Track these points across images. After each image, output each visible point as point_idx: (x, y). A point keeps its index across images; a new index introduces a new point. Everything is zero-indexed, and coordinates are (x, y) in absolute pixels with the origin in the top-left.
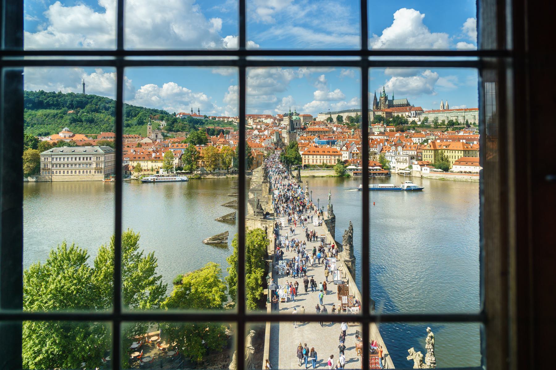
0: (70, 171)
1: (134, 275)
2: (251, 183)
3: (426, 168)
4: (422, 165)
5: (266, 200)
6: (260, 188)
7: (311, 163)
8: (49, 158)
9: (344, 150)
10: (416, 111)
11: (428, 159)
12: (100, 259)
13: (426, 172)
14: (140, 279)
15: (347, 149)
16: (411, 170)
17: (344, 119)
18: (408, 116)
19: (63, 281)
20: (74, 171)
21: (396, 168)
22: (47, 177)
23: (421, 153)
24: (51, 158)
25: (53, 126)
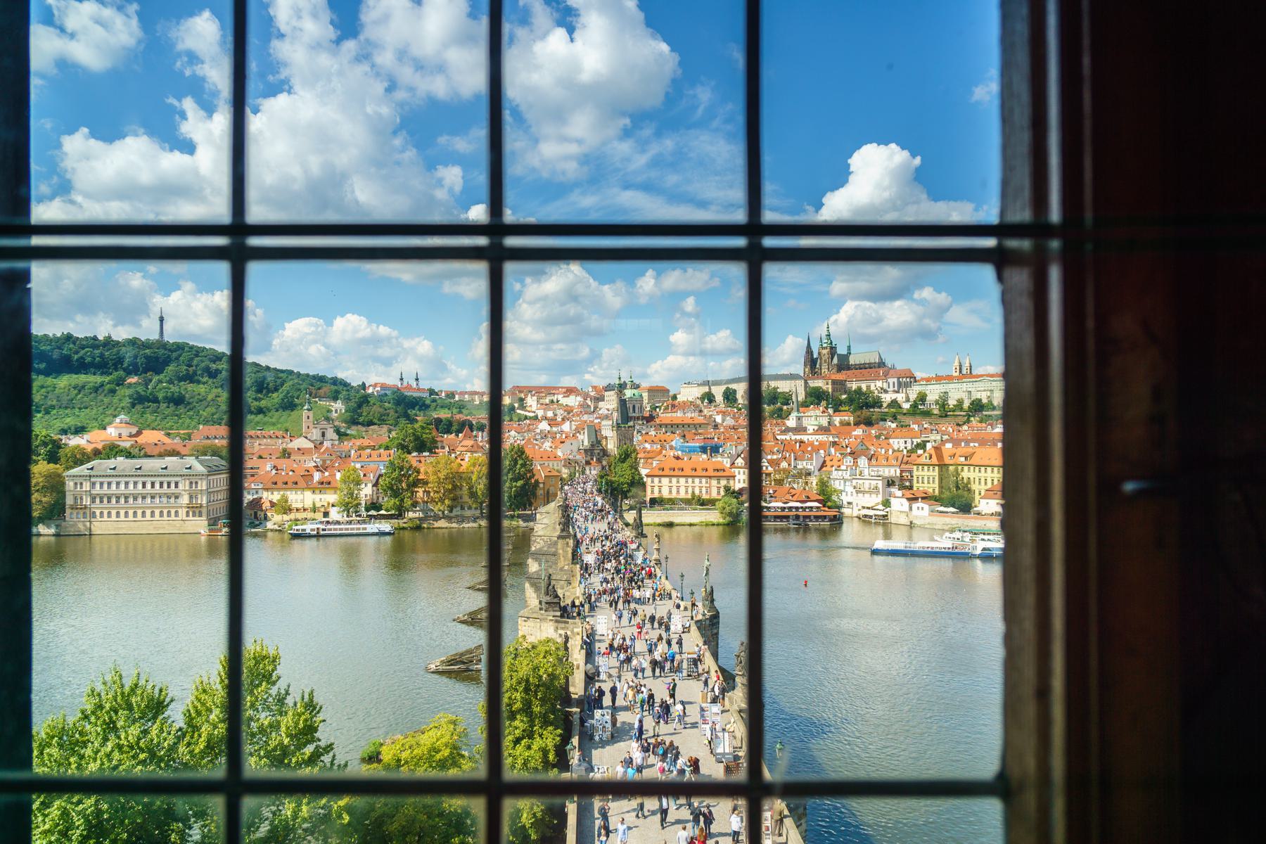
0: (131, 512)
1: (272, 744)
2: (533, 539)
3: (920, 504)
4: (913, 499)
5: (565, 577)
6: (554, 550)
7: (665, 494)
8: (84, 484)
9: (740, 465)
10: (899, 378)
11: (926, 485)
12: (195, 707)
13: (920, 513)
14: (285, 751)
16: (888, 509)
18: (882, 389)
19: (116, 755)
20: (139, 512)
21: (854, 504)
22: (81, 526)
23: (911, 472)
24: (88, 484)
25: (94, 411)
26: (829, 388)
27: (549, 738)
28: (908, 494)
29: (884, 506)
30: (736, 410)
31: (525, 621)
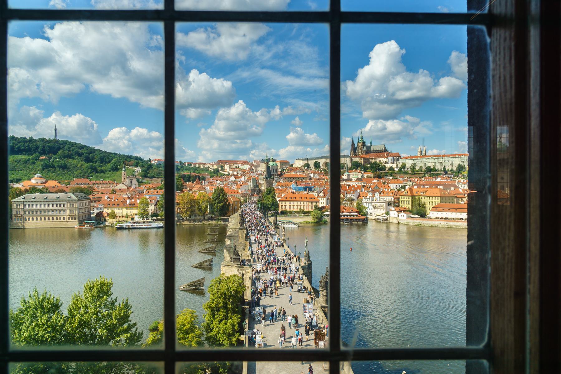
0: (43, 218)
1: (108, 324)
3: (403, 214)
5: (242, 247)
6: (237, 234)
7: (288, 209)
8: (21, 205)
9: (321, 196)
10: (393, 157)
11: (405, 205)
12: (73, 307)
13: (403, 218)
14: (114, 326)
15: (324, 195)
16: (388, 216)
17: (321, 165)
18: (386, 162)
19: (37, 329)
20: (47, 218)
21: (373, 214)
22: (20, 225)
23: (399, 199)
24: (23, 205)
25: (25, 172)
26: (362, 161)
27: (235, 320)
28: (397, 209)
29: (386, 214)
30: (319, 172)
31: (224, 267)
